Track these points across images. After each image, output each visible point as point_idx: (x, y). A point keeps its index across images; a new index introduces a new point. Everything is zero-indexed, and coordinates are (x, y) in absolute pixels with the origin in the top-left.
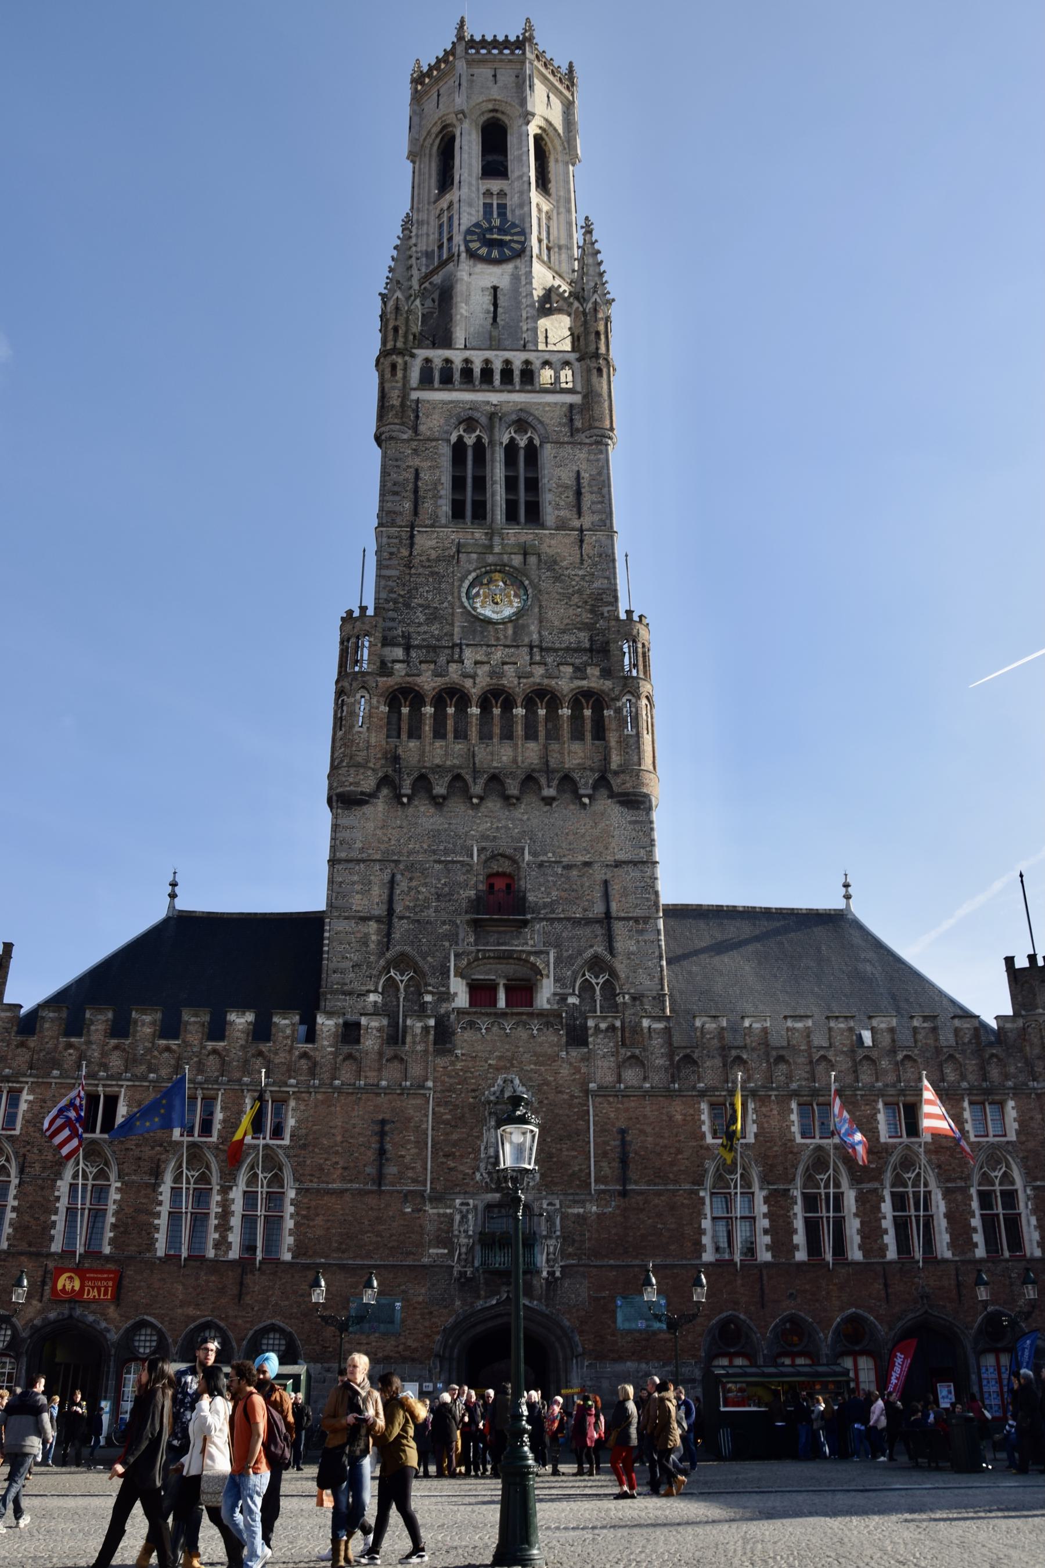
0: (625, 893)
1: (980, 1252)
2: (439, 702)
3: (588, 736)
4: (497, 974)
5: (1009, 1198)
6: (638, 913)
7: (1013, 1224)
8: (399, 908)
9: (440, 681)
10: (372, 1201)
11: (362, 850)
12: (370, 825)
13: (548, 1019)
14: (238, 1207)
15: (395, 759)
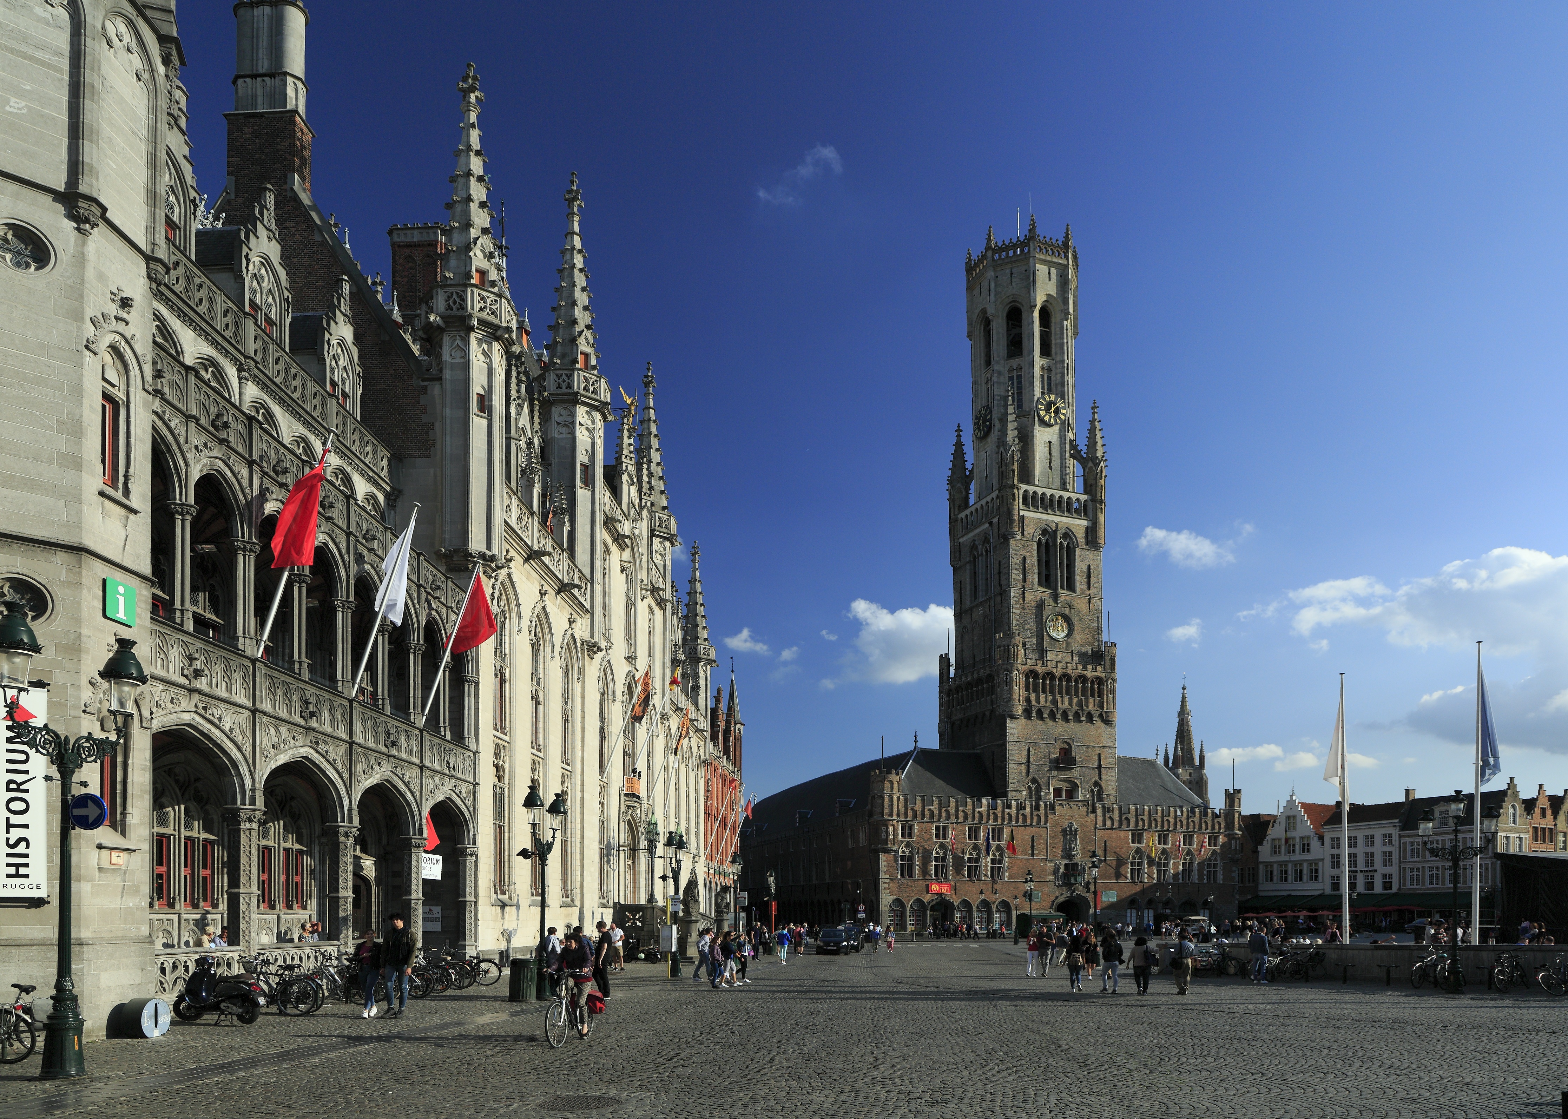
0: (1106, 758)
1: (1205, 881)
2: (1044, 679)
3: (1096, 695)
4: (1064, 786)
5: (1215, 865)
6: (1110, 766)
7: (1215, 872)
8: (1031, 759)
9: (1044, 669)
10: (1031, 861)
11: (1018, 737)
12: (1020, 727)
13: (1085, 803)
14: (989, 864)
15: (1028, 700)
